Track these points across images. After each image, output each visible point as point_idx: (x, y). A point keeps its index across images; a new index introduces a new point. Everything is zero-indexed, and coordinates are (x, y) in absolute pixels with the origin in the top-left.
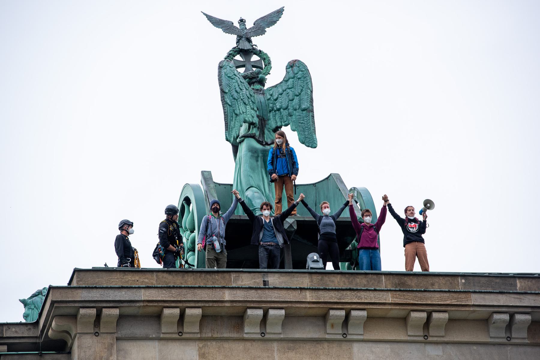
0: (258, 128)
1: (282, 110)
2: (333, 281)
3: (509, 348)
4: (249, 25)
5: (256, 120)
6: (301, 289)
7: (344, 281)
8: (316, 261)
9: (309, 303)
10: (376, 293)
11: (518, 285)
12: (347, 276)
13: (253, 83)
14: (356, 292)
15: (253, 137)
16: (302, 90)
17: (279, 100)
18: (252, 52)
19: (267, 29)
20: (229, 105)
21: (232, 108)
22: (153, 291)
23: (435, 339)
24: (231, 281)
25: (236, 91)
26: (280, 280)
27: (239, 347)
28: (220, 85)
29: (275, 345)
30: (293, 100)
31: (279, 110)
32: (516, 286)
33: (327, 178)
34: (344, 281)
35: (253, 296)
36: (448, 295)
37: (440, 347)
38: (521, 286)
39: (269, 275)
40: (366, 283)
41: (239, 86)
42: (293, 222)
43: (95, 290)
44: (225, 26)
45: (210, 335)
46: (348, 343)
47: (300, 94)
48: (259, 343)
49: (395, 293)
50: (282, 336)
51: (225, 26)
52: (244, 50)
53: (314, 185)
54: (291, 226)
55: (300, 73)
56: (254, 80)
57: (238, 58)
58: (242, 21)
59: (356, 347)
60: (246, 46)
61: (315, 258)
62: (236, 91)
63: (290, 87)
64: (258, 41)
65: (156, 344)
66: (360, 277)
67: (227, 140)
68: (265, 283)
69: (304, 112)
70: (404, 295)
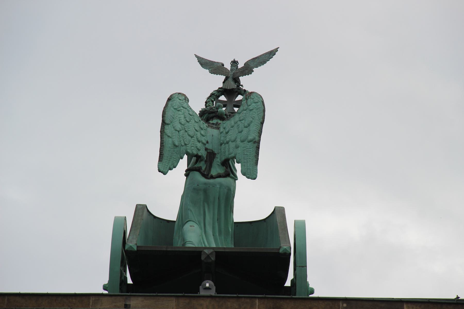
0: (206, 161)
1: (230, 143)
2: (201, 305)
4: (241, 65)
8: (208, 289)
12: (217, 299)
13: (212, 118)
15: (198, 170)
16: (252, 122)
17: (230, 133)
18: (236, 92)
19: (255, 69)
20: (169, 136)
21: (170, 140)
24: (89, 304)
25: (180, 123)
28: (163, 117)
30: (241, 132)
31: (228, 143)
33: (273, 212)
39: (132, 298)
40: (237, 307)
41: (185, 118)
42: (211, 253)
44: (214, 68)
51: (214, 68)
52: (232, 90)
53: (264, 220)
55: (254, 104)
56: (214, 115)
57: (223, 98)
58: (235, 63)
60: (233, 85)
61: (207, 285)
62: (180, 123)
63: (241, 119)
64: (246, 82)
67: (159, 171)
69: (250, 144)
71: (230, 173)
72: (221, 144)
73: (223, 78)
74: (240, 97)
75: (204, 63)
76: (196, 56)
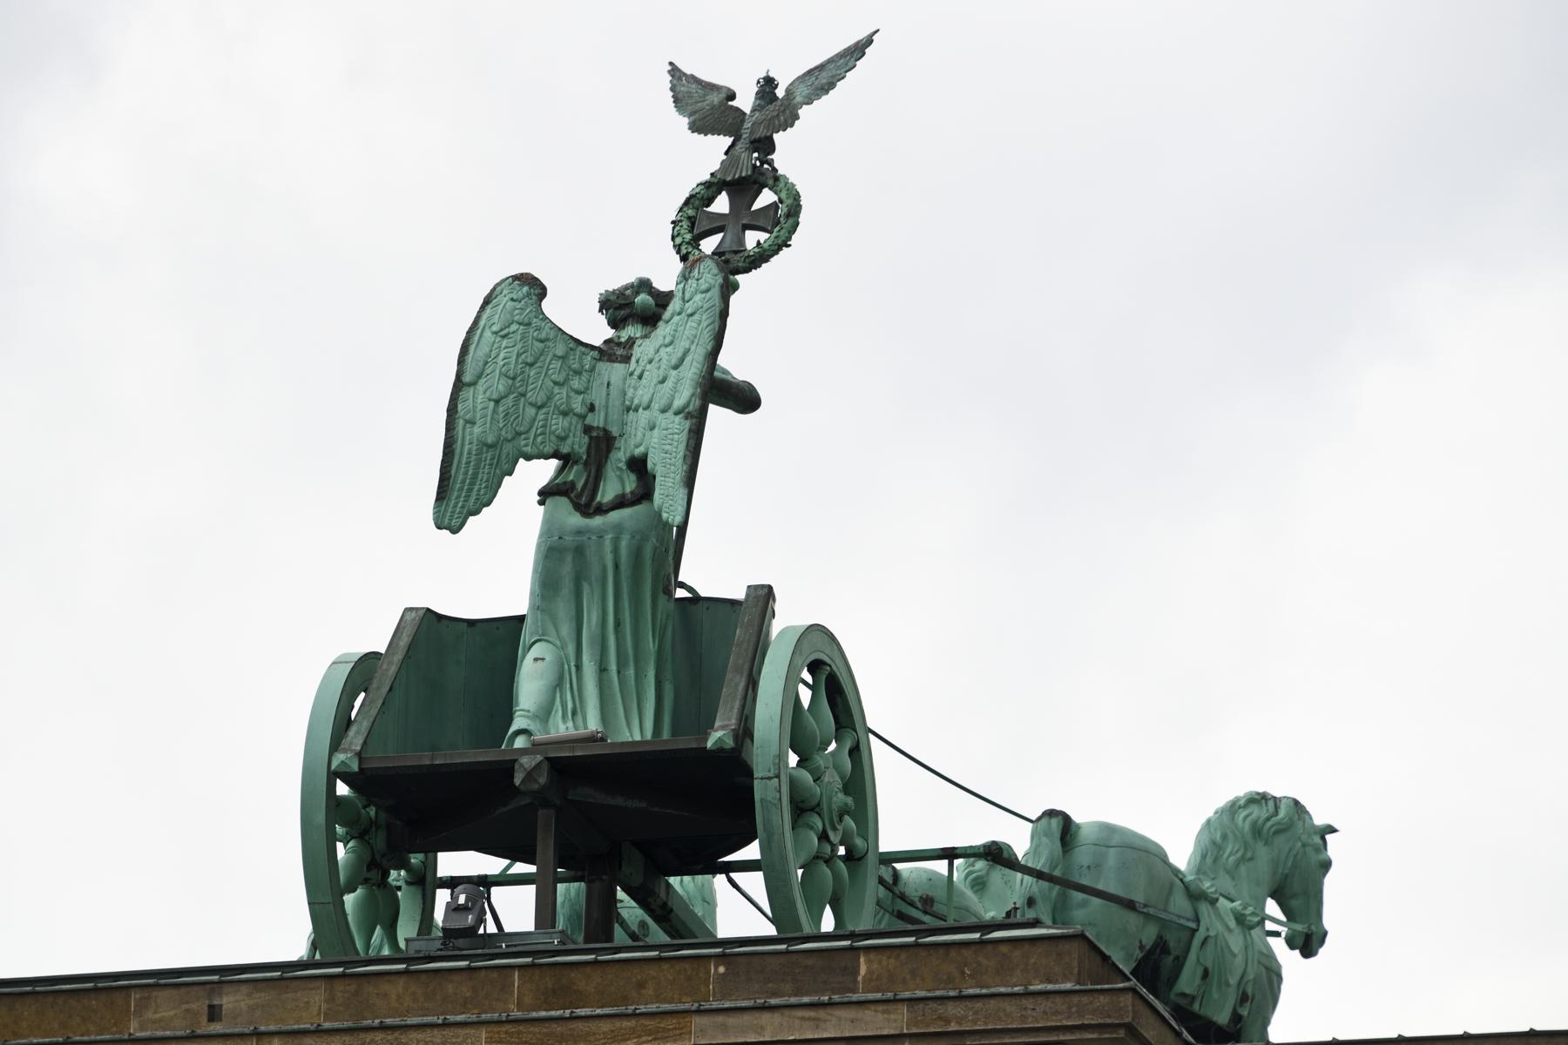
0: (586, 464)
2: (386, 995)
7: (414, 993)
10: (448, 1032)
11: (863, 970)
14: (396, 1034)
24: (128, 1010)
26: (251, 1002)
30: (662, 382)
32: (857, 973)
34: (414, 993)
36: (631, 1023)
38: (869, 972)
39: (226, 988)
42: (538, 765)
47: (682, 360)
49: (495, 1029)
51: (704, 106)
54: (530, 775)
58: (768, 84)
66: (456, 978)
67: (439, 527)
68: (214, 1014)
70: (519, 1033)
72: (629, 409)
74: (766, 198)
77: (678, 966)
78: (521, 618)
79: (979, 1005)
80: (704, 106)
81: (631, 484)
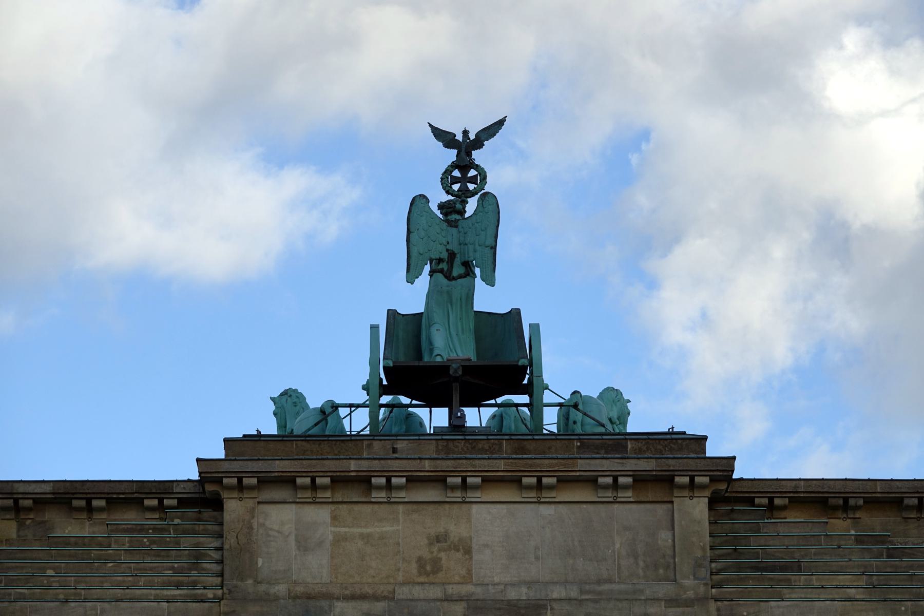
3: (616, 506)
4: (472, 136)
5: (445, 255)
6: (420, 459)
9: (428, 471)
11: (629, 446)
13: (450, 213)
15: (441, 271)
22: (286, 462)
23: (547, 500)
27: (367, 509)
29: (401, 508)
35: (376, 465)
36: (556, 461)
37: (553, 506)
43: (235, 462)
45: (340, 500)
46: (468, 505)
48: (387, 505)
50: (406, 500)
52: (464, 164)
54: (456, 371)
58: (466, 133)
59: (475, 508)
65: (294, 506)
68: (395, 450)
71: (469, 273)
73: (455, 151)
74: (472, 173)
75: (440, 134)
76: (430, 125)
77: (563, 442)
78: (422, 313)
79: (680, 461)
80: (444, 137)
81: (462, 270)
